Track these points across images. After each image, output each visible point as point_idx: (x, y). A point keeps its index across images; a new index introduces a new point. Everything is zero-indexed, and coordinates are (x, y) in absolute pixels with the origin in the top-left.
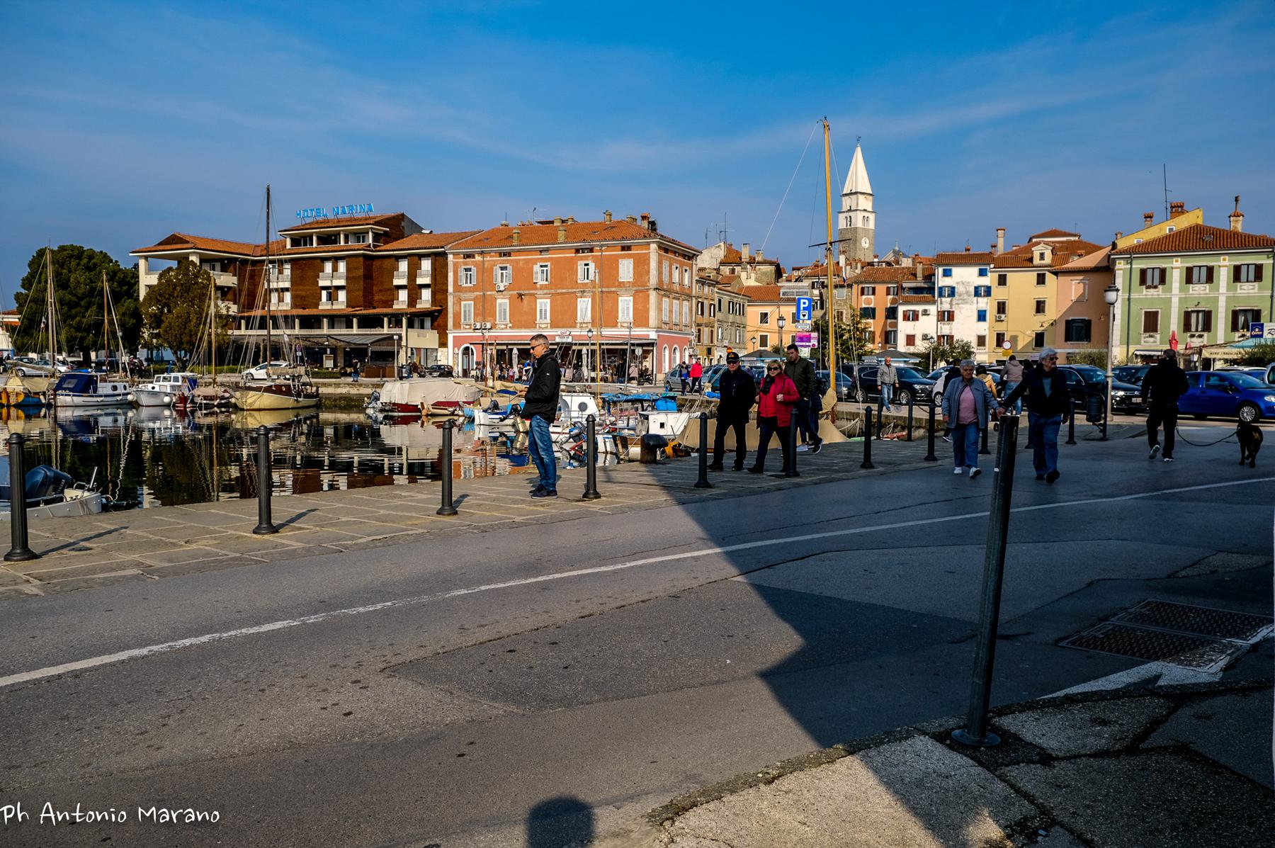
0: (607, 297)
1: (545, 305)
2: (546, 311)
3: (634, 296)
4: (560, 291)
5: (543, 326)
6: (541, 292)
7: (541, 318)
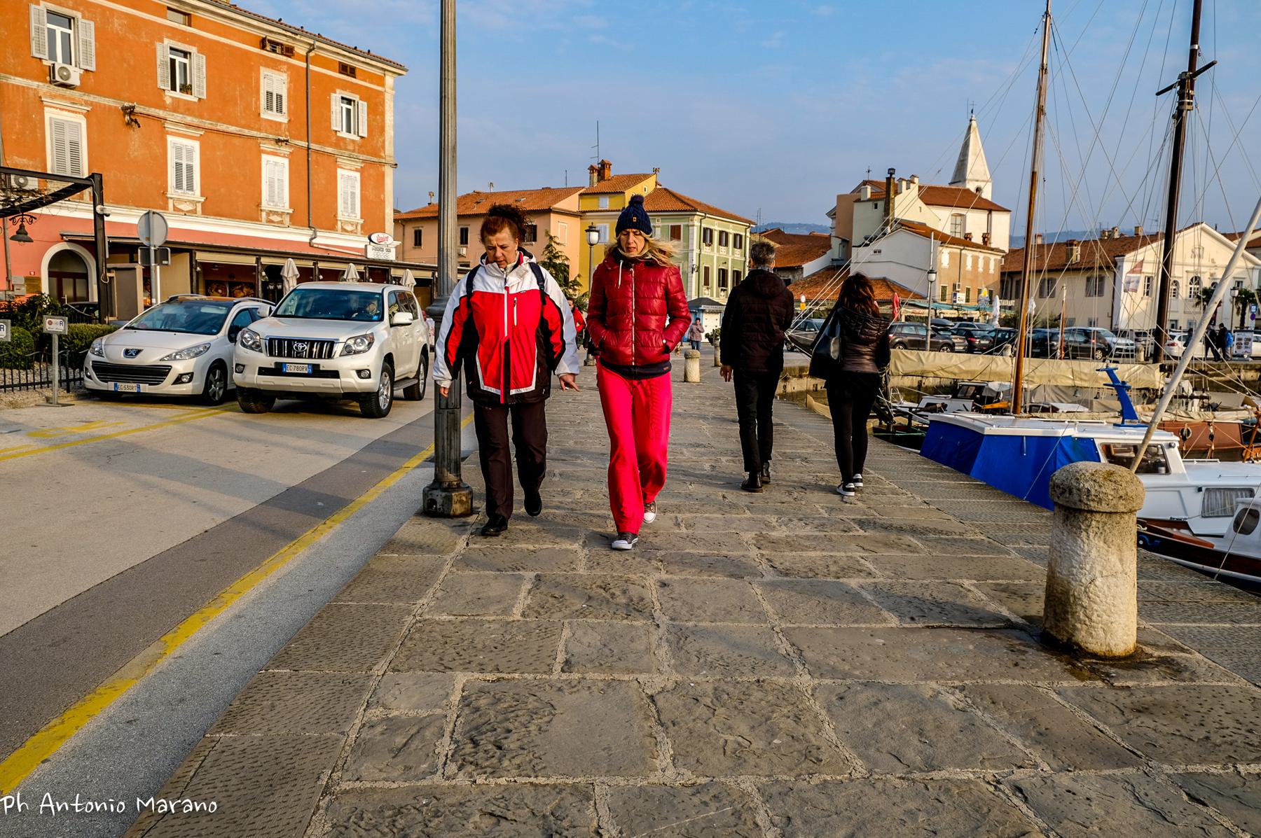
0: (317, 163)
1: (190, 152)
2: (190, 168)
3: (361, 171)
4: (223, 127)
6: (178, 117)
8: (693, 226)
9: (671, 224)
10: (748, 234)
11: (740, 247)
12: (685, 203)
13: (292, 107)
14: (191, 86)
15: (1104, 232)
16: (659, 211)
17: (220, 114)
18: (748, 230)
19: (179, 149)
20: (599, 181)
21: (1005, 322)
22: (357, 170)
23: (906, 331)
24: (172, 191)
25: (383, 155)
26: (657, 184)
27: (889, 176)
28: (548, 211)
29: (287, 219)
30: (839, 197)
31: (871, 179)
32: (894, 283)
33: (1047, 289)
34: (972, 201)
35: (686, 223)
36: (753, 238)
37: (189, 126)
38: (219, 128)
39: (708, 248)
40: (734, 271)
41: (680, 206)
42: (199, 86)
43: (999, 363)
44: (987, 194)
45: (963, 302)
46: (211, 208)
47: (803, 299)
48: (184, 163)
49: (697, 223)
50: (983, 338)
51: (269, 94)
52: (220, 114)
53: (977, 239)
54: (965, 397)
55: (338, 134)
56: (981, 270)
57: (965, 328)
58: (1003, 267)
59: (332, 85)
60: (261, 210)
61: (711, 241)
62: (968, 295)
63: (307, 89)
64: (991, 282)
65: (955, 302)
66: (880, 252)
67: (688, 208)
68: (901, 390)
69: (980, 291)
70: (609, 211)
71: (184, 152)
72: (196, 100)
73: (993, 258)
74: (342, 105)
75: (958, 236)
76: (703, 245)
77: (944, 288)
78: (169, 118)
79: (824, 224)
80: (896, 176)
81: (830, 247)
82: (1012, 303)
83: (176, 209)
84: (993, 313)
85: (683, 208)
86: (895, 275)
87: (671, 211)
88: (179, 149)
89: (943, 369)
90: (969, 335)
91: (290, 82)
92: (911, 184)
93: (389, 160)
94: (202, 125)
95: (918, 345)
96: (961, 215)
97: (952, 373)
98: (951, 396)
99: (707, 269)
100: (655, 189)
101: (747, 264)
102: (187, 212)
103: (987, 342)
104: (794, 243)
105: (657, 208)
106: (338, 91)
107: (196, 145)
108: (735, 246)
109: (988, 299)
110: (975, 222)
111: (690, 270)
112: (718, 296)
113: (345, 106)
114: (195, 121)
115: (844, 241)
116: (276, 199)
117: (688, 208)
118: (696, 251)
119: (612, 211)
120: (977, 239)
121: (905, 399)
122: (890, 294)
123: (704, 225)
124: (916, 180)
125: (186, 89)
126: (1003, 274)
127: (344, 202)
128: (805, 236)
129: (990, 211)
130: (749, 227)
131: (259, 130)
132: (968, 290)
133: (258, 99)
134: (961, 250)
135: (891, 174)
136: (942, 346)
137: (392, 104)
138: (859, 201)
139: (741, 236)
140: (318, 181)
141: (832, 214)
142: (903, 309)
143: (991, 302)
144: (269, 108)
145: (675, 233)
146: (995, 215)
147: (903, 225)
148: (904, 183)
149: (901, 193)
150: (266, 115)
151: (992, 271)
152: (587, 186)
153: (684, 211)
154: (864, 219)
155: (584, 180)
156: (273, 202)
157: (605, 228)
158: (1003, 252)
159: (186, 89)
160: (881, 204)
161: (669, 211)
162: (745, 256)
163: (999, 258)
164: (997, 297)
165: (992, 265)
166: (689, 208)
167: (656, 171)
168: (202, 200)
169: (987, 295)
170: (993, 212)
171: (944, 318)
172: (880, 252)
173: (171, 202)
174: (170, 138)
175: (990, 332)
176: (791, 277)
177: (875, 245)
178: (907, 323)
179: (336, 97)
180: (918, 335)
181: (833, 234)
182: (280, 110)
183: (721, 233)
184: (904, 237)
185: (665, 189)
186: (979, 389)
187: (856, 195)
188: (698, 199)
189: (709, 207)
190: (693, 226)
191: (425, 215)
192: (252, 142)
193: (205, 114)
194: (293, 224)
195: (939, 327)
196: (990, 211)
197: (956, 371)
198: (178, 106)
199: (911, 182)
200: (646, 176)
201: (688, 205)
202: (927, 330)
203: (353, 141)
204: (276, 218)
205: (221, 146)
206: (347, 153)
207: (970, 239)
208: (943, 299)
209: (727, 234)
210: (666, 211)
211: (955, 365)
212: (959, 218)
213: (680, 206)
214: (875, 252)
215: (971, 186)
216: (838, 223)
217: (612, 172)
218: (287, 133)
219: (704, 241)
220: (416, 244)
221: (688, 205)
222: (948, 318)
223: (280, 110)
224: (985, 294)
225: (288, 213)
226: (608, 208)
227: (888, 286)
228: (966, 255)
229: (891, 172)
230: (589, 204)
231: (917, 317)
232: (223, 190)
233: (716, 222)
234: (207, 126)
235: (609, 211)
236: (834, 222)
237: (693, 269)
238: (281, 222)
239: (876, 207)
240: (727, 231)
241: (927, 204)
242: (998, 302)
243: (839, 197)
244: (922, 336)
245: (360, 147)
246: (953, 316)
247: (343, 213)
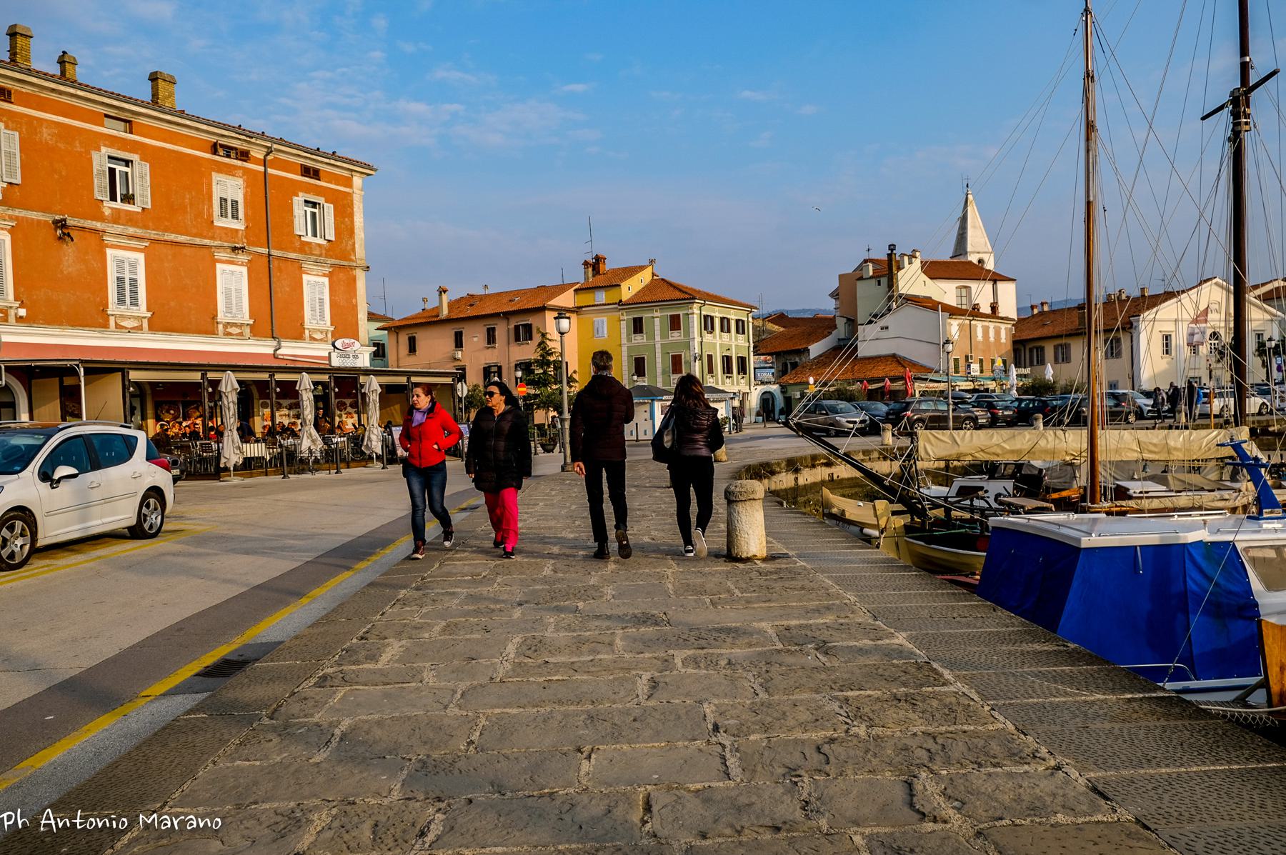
0: (280, 270)
1: (133, 265)
2: (134, 282)
3: (330, 276)
5: (128, 324)
6: (119, 229)
7: (121, 301)
8: (693, 314)
9: (669, 314)
10: (750, 319)
11: (744, 333)
12: (683, 292)
13: (250, 213)
14: (133, 195)
15: (1110, 295)
16: (657, 302)
17: (166, 223)
18: (750, 315)
19: (120, 263)
20: (594, 276)
21: (1023, 390)
22: (324, 275)
23: (923, 407)
24: (113, 307)
25: (353, 258)
26: (653, 275)
27: (890, 252)
28: (543, 309)
29: (247, 331)
30: (841, 277)
31: (872, 257)
32: (904, 359)
33: (1063, 356)
34: (976, 272)
35: (686, 312)
36: (756, 323)
37: (131, 237)
38: (166, 238)
39: (709, 335)
40: (738, 357)
41: (678, 295)
42: (142, 196)
43: (1050, 439)
44: (990, 265)
45: (978, 373)
46: (158, 324)
47: (811, 380)
48: (127, 276)
49: (696, 311)
50: (1006, 408)
51: (223, 200)
52: (166, 223)
53: (985, 309)
54: (1003, 477)
55: (303, 239)
56: (992, 339)
57: (984, 399)
58: (1014, 335)
59: (295, 188)
60: (217, 323)
61: (713, 328)
62: (981, 366)
63: (266, 193)
64: (1003, 352)
65: (969, 373)
66: (887, 328)
67: (687, 296)
68: (927, 472)
69: (993, 362)
70: (605, 305)
71: (127, 265)
72: (139, 210)
73: (1003, 327)
74: (306, 208)
75: (964, 307)
76: (704, 332)
77: (956, 360)
78: (109, 230)
79: (828, 306)
80: (898, 252)
81: (835, 327)
82: (1027, 371)
83: (118, 326)
84: (1009, 383)
85: (682, 297)
86: (905, 350)
87: (670, 300)
88: (120, 263)
89: (982, 450)
90: (991, 407)
91: (247, 187)
92: (914, 259)
93: (359, 263)
94: (147, 236)
95: (937, 423)
96: (966, 287)
97: (994, 454)
98: (987, 477)
99: (710, 357)
100: (653, 279)
101: (752, 349)
102: (131, 328)
103: (1011, 413)
104: (798, 326)
105: (654, 298)
106: (301, 194)
107: (140, 257)
108: (737, 332)
109: (1003, 369)
110: (982, 293)
111: (693, 359)
112: (723, 383)
113: (309, 210)
114: (139, 232)
115: (849, 320)
116: (234, 310)
117: (687, 296)
118: (698, 339)
119: (608, 304)
120: (985, 309)
121: (934, 483)
122: (901, 369)
123: (703, 313)
124: (918, 254)
125: (128, 198)
126: (1015, 343)
127: (312, 310)
128: (810, 318)
129: (995, 281)
130: (751, 312)
131: (212, 238)
132: (981, 361)
133: (211, 206)
134: (970, 321)
135: (892, 250)
136: (965, 420)
137: (361, 206)
138: (861, 278)
139: (743, 322)
140: (281, 288)
141: (835, 295)
142: (916, 384)
143: (1006, 371)
144: (223, 214)
145: (675, 323)
146: (1000, 285)
147: (908, 300)
148: (906, 258)
149: (903, 268)
150: (220, 223)
151: (1003, 340)
152: (582, 281)
153: (682, 299)
154: (868, 296)
155: (578, 275)
156: (231, 313)
157: (603, 322)
158: (1013, 320)
159: (128, 198)
160: (884, 281)
161: (667, 301)
162: (749, 342)
163: (1010, 326)
164: (1013, 365)
165: (1003, 334)
166: (688, 296)
167: (652, 262)
168: (149, 315)
169: (1002, 365)
170: (998, 282)
171: (960, 390)
172: (887, 328)
173: (112, 320)
174: (109, 252)
175: (1013, 402)
176: (797, 359)
177: (883, 322)
178: (922, 398)
179: (298, 201)
180: (938, 411)
181: (838, 314)
182: (235, 216)
183: (722, 319)
184: (910, 311)
185: (663, 279)
186: (1019, 466)
187: (858, 274)
188: (697, 287)
189: (708, 294)
190: (693, 314)
191: (414, 322)
192: (205, 251)
193: (151, 224)
194: (254, 336)
195: (959, 400)
196: (995, 281)
197: (999, 451)
198: (119, 218)
199: (912, 256)
200: (642, 268)
201: (686, 293)
202: (948, 405)
203: (319, 245)
204: (234, 330)
205: (170, 257)
206: (313, 258)
207: (978, 310)
208: (957, 371)
209: (728, 320)
210: (664, 301)
211: (998, 445)
212: (964, 291)
213: (678, 295)
214: (882, 329)
215: (973, 258)
216: (842, 303)
217: (608, 266)
218: (245, 240)
219: (706, 328)
220: (410, 351)
221: (686, 293)
222: (963, 390)
223: (235, 216)
224: (999, 363)
225: (248, 324)
226: (604, 302)
227: (898, 361)
228: (976, 326)
229: (892, 247)
230: (585, 299)
231: (932, 392)
232: (172, 304)
233: (717, 308)
234: (153, 237)
235: (605, 305)
236: (838, 303)
237: (696, 358)
238: (241, 334)
239: (879, 284)
240: (729, 317)
241: (931, 278)
242: (1014, 371)
243: (841, 277)
244: (943, 411)
245: (327, 251)
246: (968, 388)
247: (309, 321)
